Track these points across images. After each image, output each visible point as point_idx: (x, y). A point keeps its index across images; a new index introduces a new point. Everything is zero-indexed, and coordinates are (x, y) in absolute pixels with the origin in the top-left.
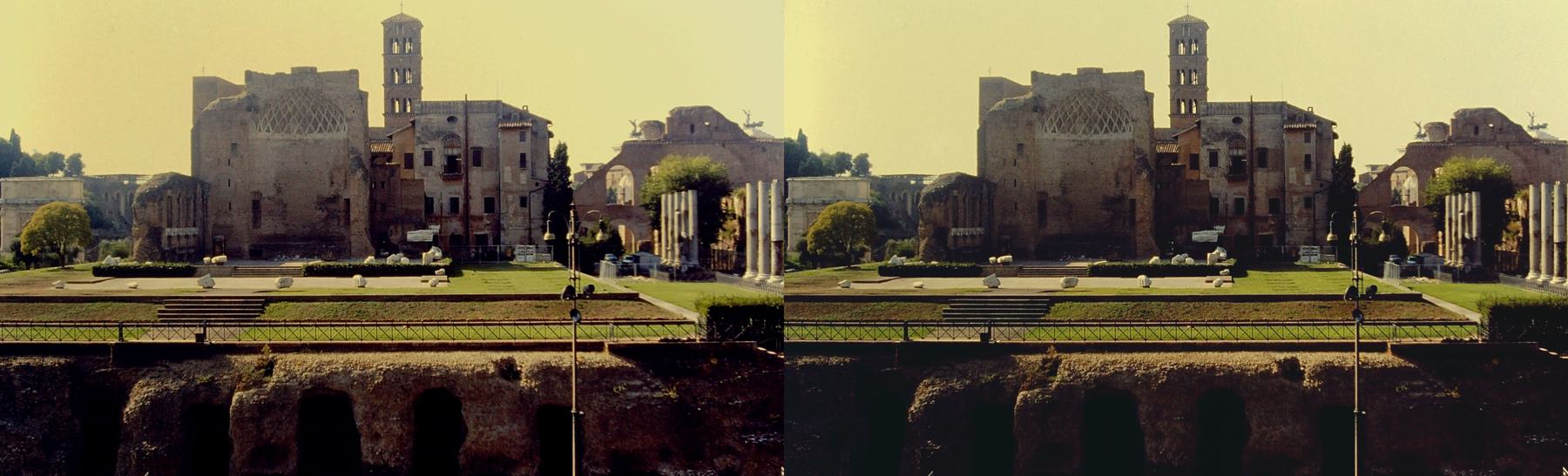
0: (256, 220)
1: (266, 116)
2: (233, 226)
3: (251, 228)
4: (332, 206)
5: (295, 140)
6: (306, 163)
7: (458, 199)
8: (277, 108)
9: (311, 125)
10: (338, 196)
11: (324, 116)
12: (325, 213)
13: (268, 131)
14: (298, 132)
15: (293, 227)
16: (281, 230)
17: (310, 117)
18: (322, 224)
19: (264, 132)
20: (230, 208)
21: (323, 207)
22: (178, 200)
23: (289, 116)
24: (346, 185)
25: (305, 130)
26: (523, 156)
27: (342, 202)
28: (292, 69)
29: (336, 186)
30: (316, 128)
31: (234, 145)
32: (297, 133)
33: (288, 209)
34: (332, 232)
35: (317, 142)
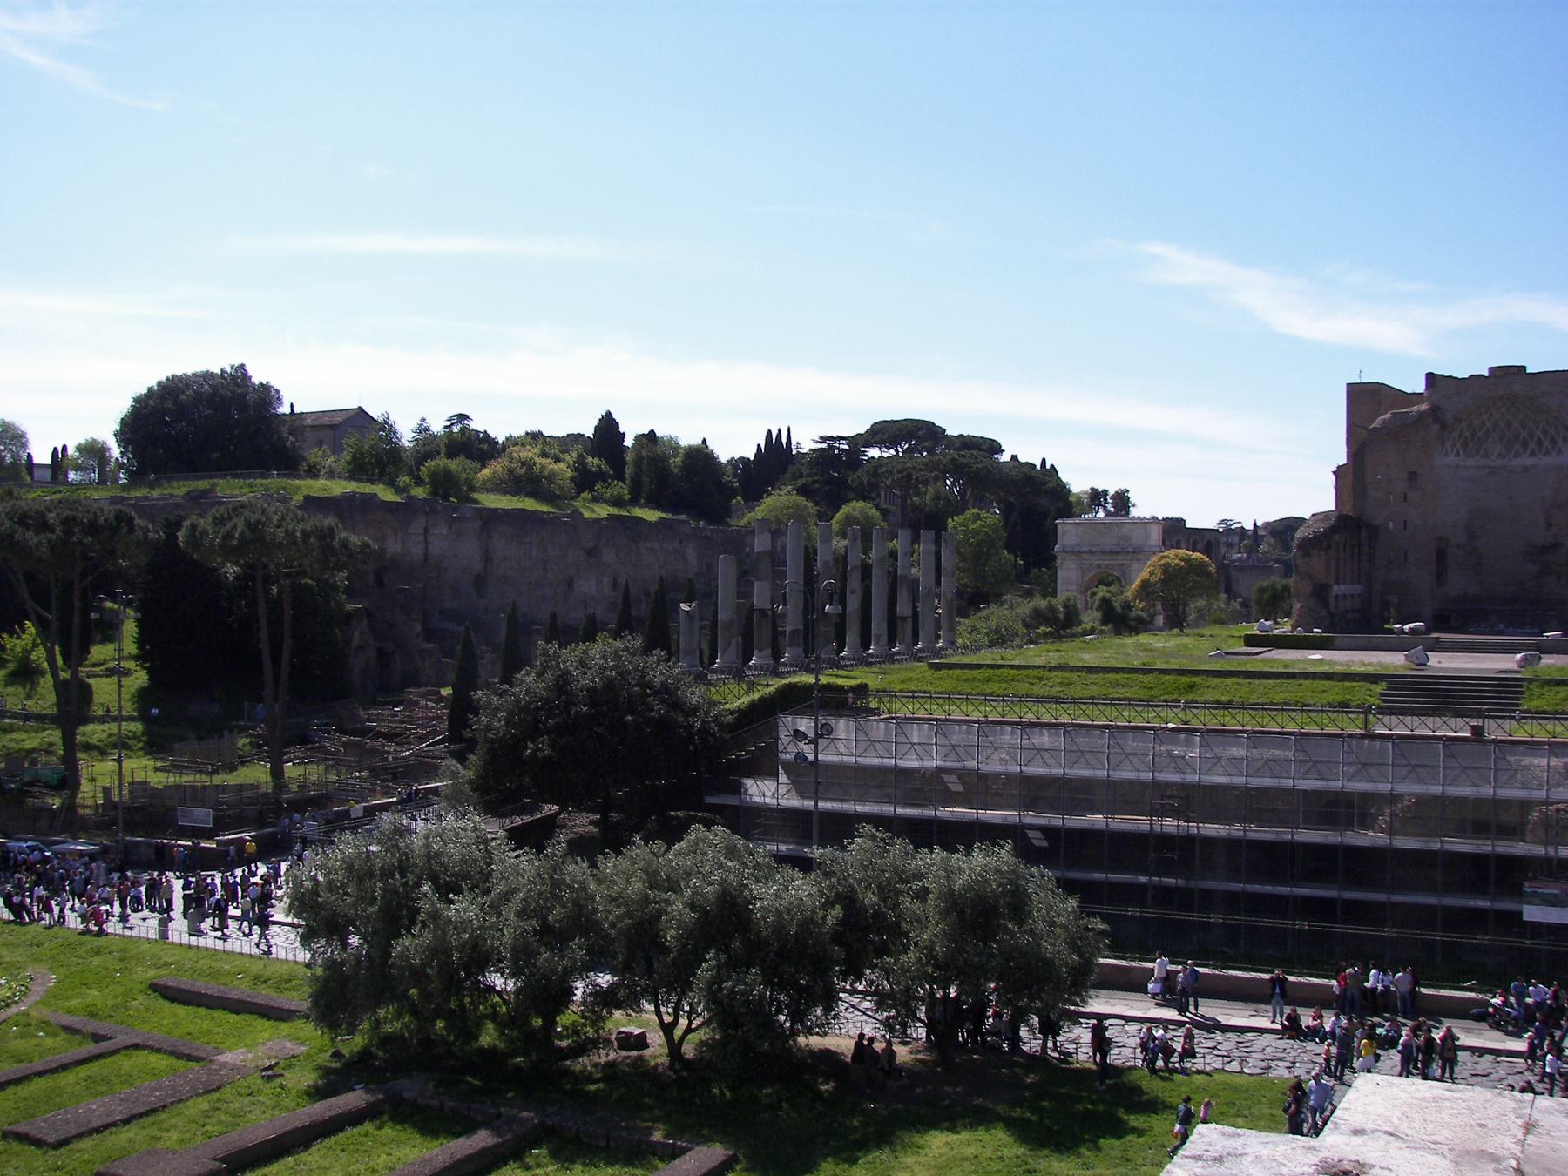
0: (1440, 576)
9: (1517, 446)
11: (1538, 433)
13: (1458, 455)
14: (1500, 455)
22: (1345, 546)
28: (1490, 368)
30: (1525, 450)
31: (1412, 476)
35: (1526, 469)
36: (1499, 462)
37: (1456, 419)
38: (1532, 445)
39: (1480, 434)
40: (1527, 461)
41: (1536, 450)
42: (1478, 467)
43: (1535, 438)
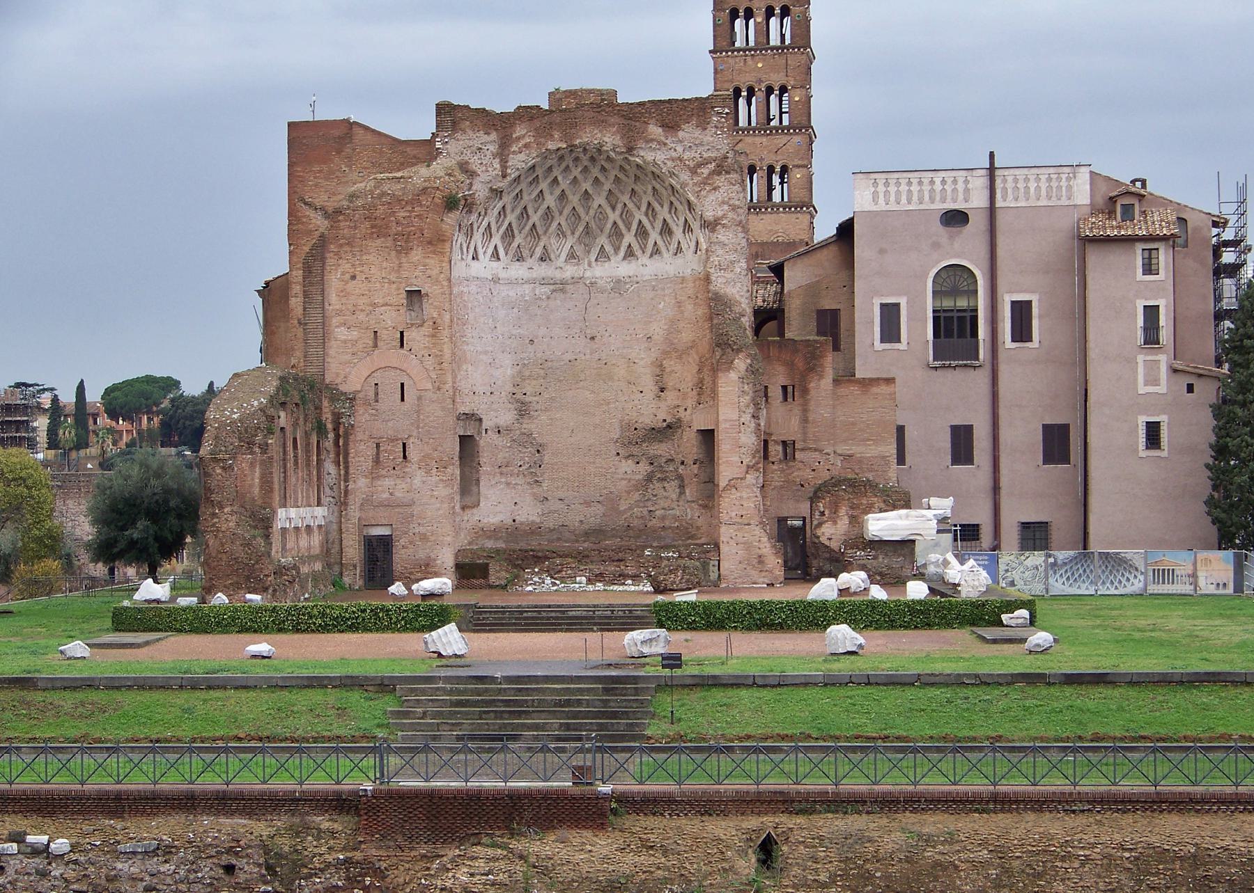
0: (468, 486)
1: (492, 217)
2: (411, 504)
3: (458, 508)
4: (661, 449)
5: (563, 283)
6: (593, 338)
7: (968, 429)
8: (518, 196)
9: (603, 240)
10: (679, 420)
11: (639, 215)
12: (644, 468)
13: (496, 256)
14: (572, 256)
15: (559, 505)
16: (529, 513)
17: (601, 216)
18: (636, 496)
19: (485, 259)
20: (405, 457)
21: (635, 450)
23: (548, 215)
24: (699, 394)
25: (589, 252)
26: (1151, 313)
27: (688, 445)
29: (671, 397)
30: (617, 249)
31: (414, 296)
32: (566, 261)
33: (546, 458)
34: (663, 518)
35: (618, 285)
36: (570, 271)
37: (491, 190)
38: (629, 238)
39: (535, 218)
40: (619, 268)
41: (636, 247)
42: (532, 281)
43: (634, 226)
